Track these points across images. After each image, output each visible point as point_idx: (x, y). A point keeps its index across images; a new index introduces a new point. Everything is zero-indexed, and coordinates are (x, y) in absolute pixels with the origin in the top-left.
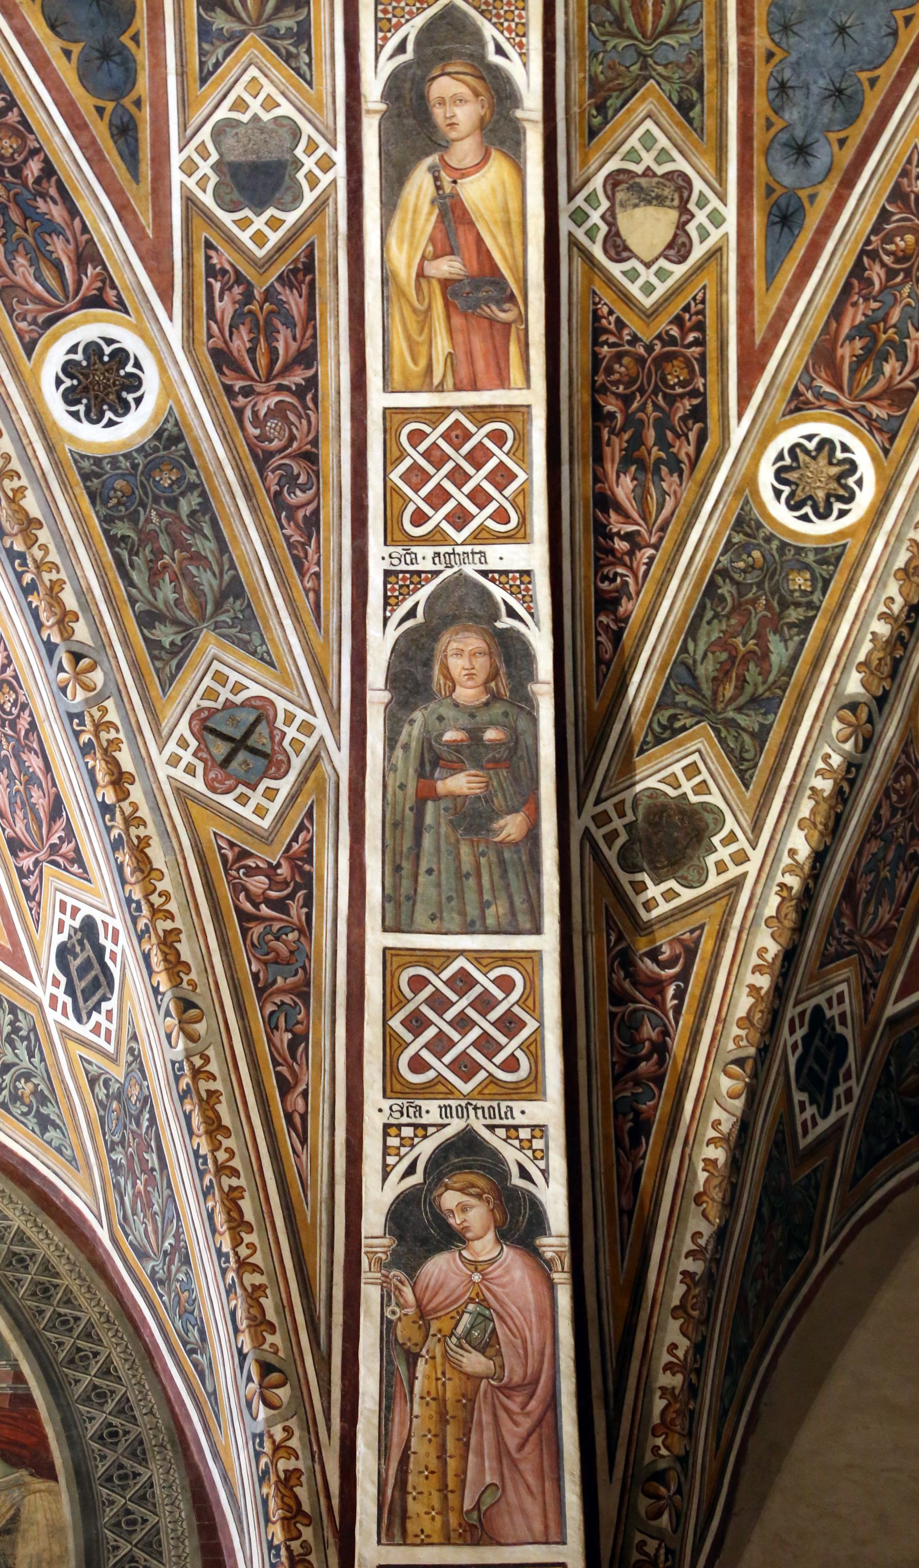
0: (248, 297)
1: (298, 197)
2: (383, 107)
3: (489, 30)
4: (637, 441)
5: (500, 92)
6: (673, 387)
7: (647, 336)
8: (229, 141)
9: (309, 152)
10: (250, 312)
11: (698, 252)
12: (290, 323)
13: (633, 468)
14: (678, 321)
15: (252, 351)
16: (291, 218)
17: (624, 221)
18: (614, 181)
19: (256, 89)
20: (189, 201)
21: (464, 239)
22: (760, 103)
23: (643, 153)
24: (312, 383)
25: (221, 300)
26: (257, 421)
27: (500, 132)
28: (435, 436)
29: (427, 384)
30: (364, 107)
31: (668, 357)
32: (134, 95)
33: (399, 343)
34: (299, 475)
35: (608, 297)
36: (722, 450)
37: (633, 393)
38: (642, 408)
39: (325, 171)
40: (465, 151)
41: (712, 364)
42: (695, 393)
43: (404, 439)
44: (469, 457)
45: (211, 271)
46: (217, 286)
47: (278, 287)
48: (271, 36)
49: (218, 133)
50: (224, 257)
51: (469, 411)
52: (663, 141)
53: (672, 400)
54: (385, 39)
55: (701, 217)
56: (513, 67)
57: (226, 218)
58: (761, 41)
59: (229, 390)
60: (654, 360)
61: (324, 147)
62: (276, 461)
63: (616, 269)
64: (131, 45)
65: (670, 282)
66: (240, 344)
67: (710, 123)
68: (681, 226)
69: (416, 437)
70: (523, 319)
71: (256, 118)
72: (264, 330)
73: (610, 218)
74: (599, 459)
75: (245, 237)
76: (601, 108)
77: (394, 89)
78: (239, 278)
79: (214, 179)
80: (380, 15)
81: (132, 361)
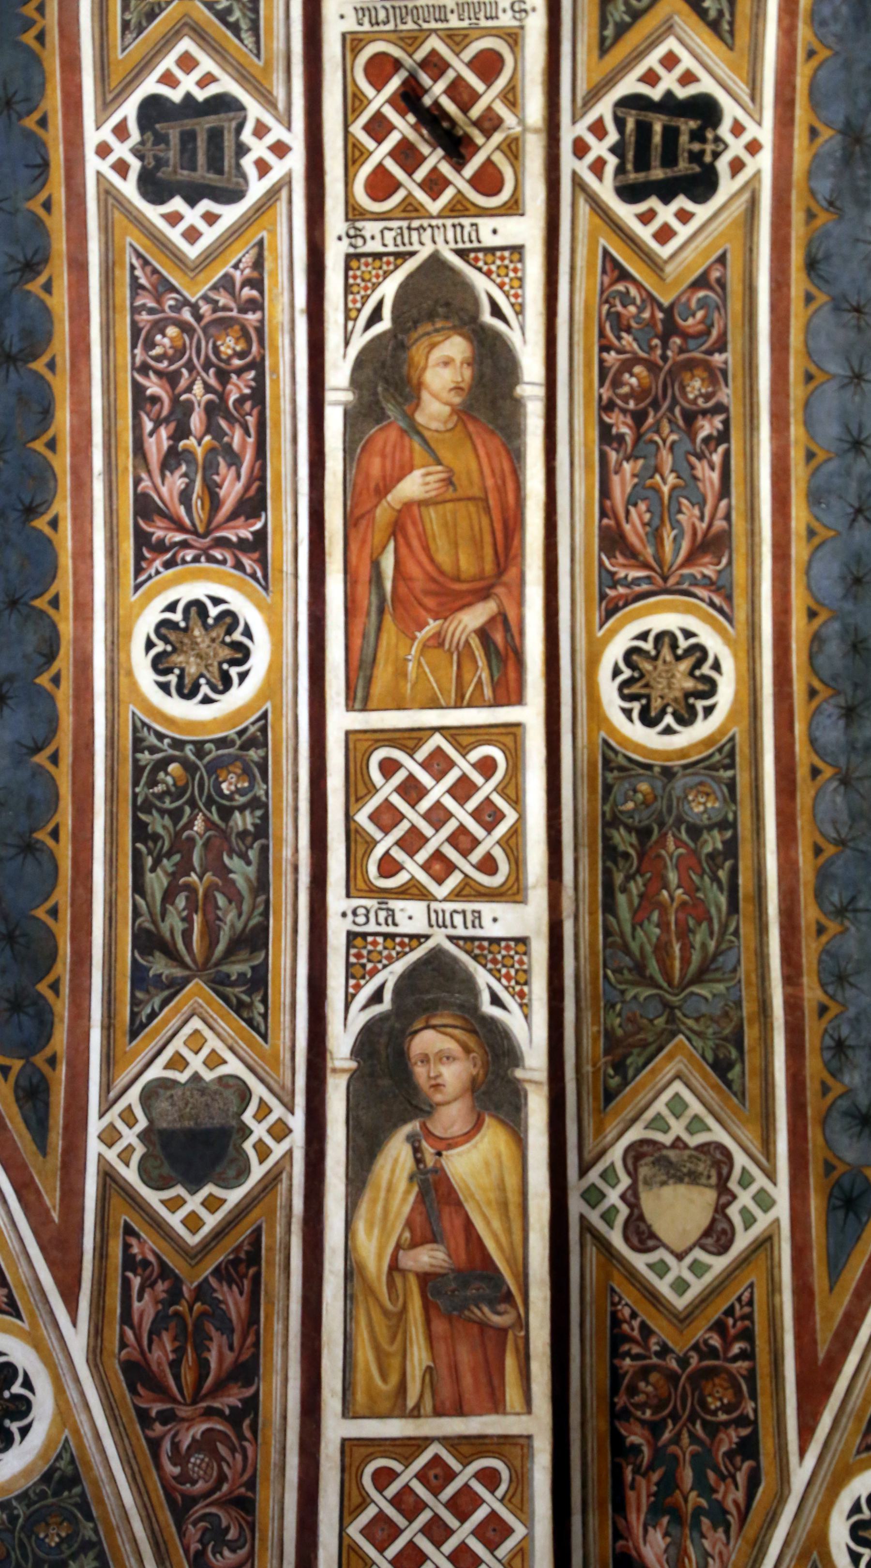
0: (175, 1294)
1: (245, 1171)
2: (353, 1065)
3: (483, 978)
4: (669, 1483)
5: (495, 1048)
6: (714, 1413)
7: (679, 1347)
8: (163, 1105)
9: (260, 1117)
10: (177, 1314)
11: (742, 1241)
12: (226, 1327)
13: (665, 1520)
14: (719, 1327)
15: (175, 1365)
16: (234, 1196)
17: (648, 1202)
18: (636, 1153)
19: (198, 1044)
20: (108, 1176)
21: (449, 1222)
22: (813, 1065)
23: (672, 1121)
24: (252, 1405)
25: (140, 1298)
26: (177, 1457)
27: (495, 1093)
28: (407, 1476)
29: (398, 1406)
30: (330, 1065)
31: (710, 1373)
32: (48, 1052)
33: (365, 1354)
34: (227, 1529)
35: (629, 1297)
36: (781, 1499)
37: (664, 1421)
38: (676, 1440)
39: (279, 1140)
40: (452, 1117)
41: (763, 1383)
42: (742, 1421)
43: (367, 1481)
44: (451, 1504)
45: (130, 1263)
46: (136, 1282)
47: (213, 1282)
48: (219, 984)
49: (148, 1097)
50: (148, 1245)
51: (453, 1443)
52: (696, 1107)
53: (713, 1429)
54: (358, 987)
55: (745, 1198)
56: (512, 1019)
57: (153, 1197)
58: (812, 992)
59: (144, 1417)
60: (689, 1378)
61: (278, 1111)
62: (199, 1510)
63: (639, 1261)
64: (49, 994)
65: (708, 1278)
66: (161, 1354)
67: (753, 1086)
68: (720, 1210)
69: (383, 1478)
70: (523, 1324)
71: (196, 1077)
72: (193, 1337)
73: (631, 1198)
74: (620, 1507)
75: (175, 1220)
76: (619, 1067)
77: (367, 1043)
78: (165, 1272)
79: (140, 1150)
80: (353, 960)
81: (20, 1380)
